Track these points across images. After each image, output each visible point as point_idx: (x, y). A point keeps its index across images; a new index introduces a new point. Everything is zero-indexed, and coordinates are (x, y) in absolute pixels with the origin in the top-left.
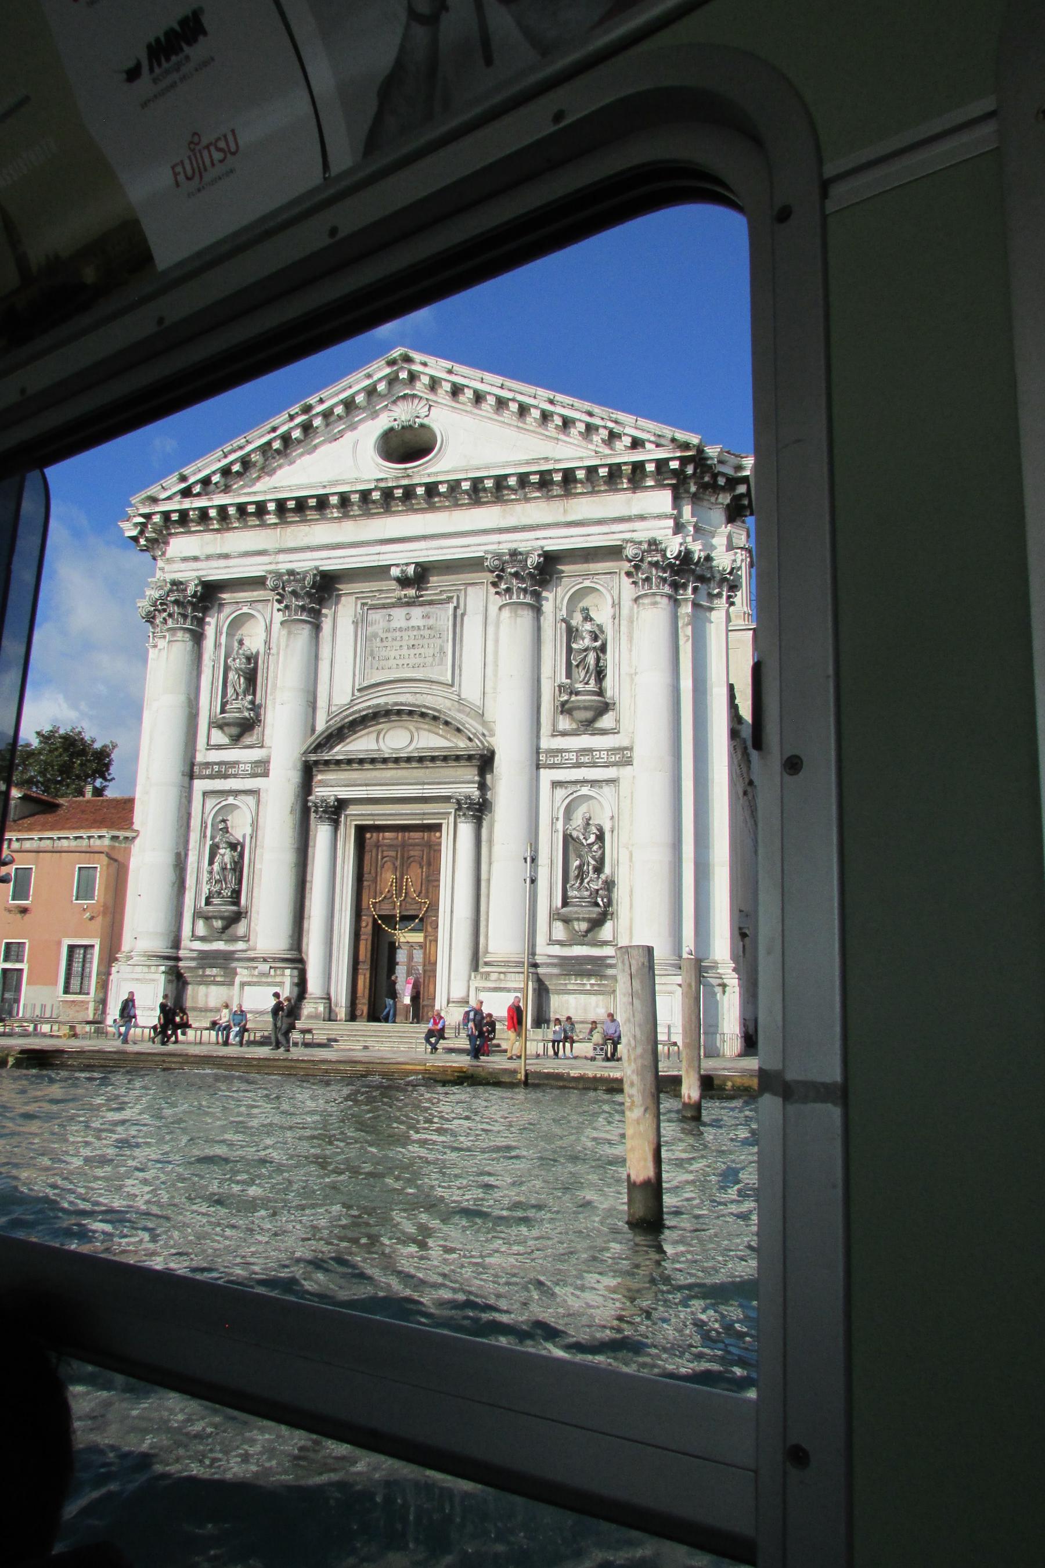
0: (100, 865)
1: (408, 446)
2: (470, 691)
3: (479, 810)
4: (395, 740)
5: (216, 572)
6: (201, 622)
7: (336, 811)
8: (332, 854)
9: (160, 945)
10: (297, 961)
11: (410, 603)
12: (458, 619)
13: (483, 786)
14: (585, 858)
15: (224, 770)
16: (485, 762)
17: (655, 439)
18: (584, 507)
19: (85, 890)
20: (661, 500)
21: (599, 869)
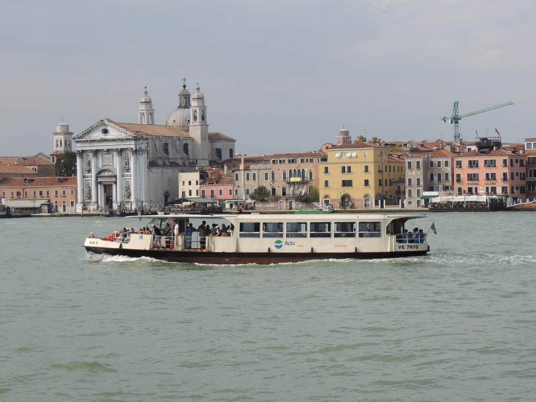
0: (74, 190)
1: (105, 131)
2: (115, 166)
3: (116, 183)
4: (106, 174)
5: (84, 149)
6: (82, 156)
7: (100, 183)
8: (101, 188)
9: (82, 201)
10: (97, 202)
11: (107, 154)
12: (113, 156)
13: (116, 179)
14: (128, 189)
15: (87, 177)
16: (116, 176)
17: (130, 134)
18: (125, 143)
19: (72, 194)
20: (133, 142)
21: (129, 189)
